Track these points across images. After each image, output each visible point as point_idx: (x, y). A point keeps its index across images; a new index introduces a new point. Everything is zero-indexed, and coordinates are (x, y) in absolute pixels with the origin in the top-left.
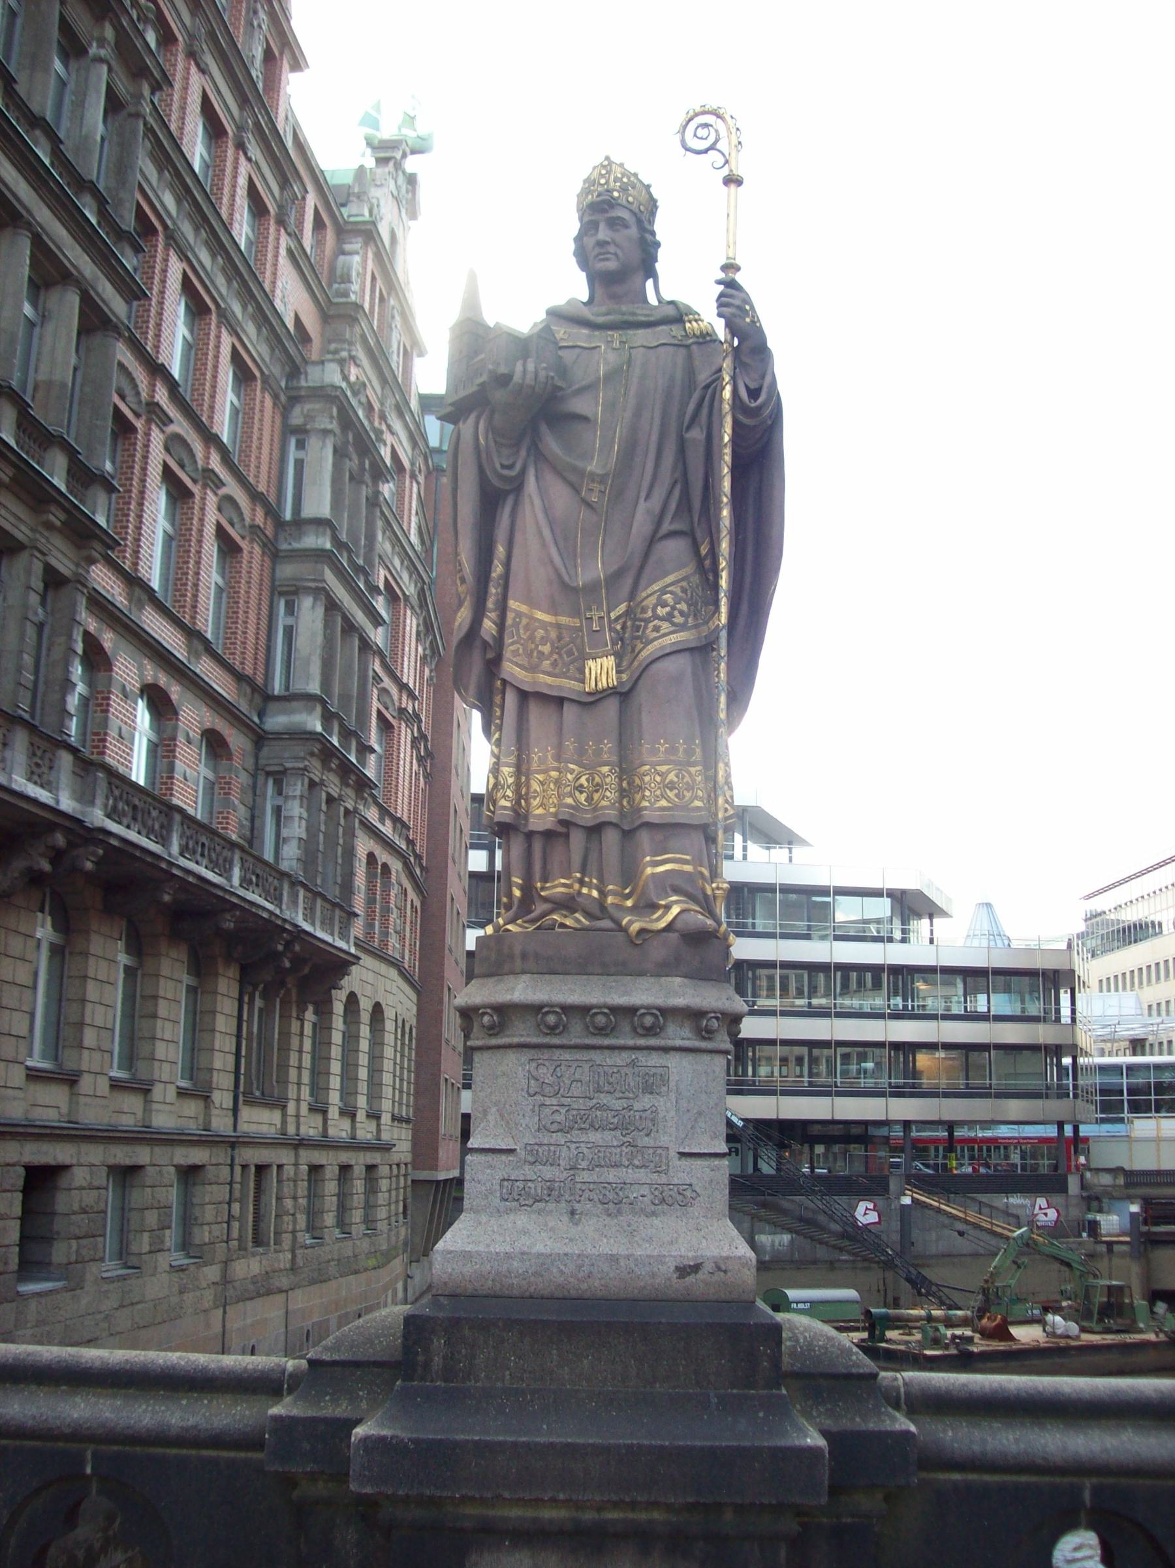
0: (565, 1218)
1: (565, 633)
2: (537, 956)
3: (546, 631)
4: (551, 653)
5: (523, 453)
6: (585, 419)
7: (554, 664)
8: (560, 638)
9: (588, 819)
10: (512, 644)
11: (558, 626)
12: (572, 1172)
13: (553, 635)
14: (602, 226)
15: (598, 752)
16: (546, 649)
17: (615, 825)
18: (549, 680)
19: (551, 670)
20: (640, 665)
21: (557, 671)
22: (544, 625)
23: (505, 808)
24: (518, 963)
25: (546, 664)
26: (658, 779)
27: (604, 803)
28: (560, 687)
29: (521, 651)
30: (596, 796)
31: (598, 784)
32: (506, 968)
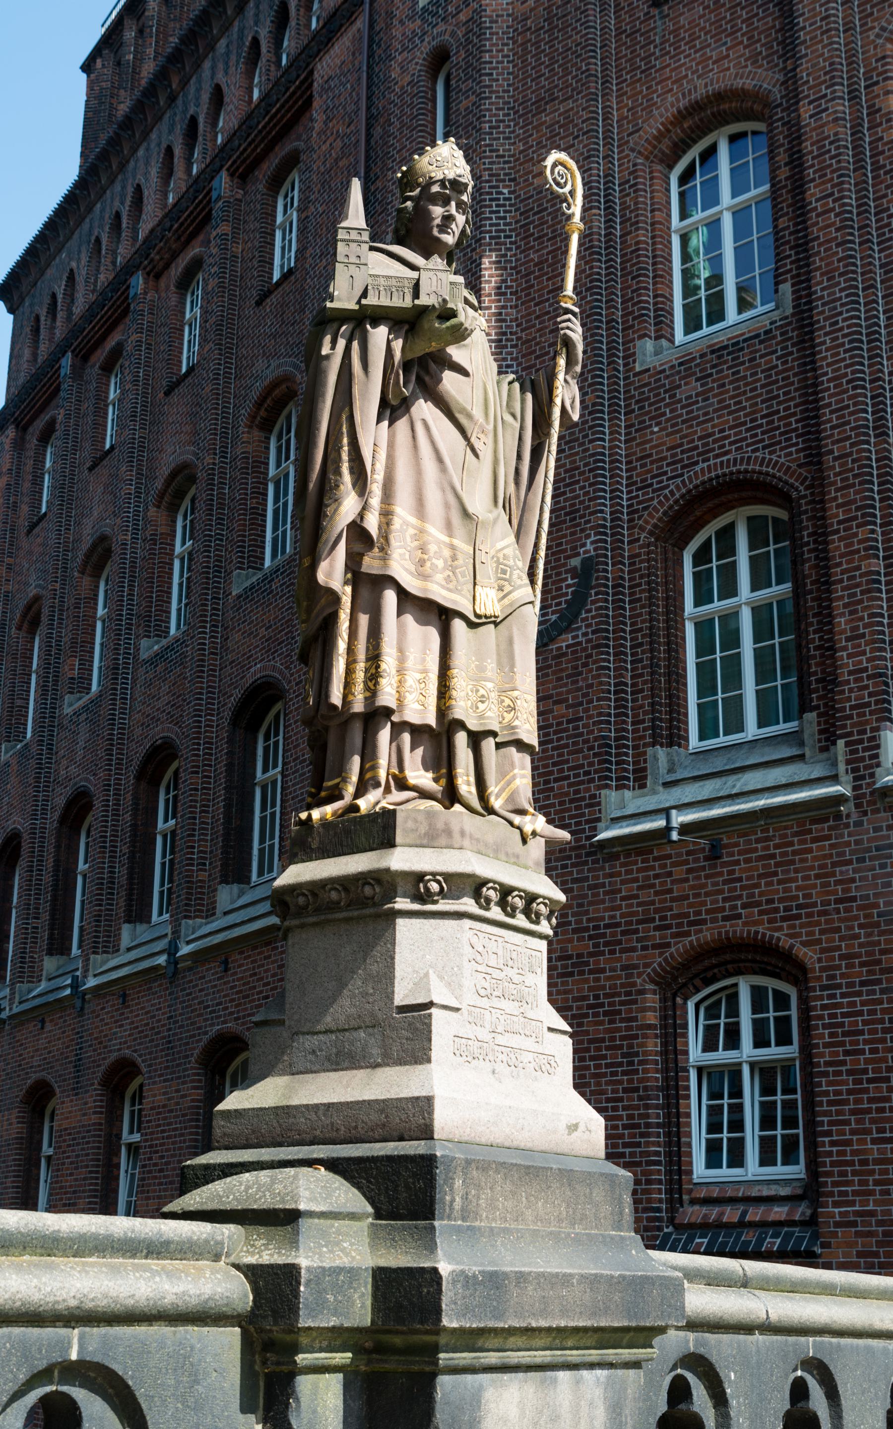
0: (491, 1075)
1: (460, 556)
2: (471, 837)
3: (439, 548)
4: (444, 569)
5: (414, 378)
6: (464, 372)
7: (448, 579)
8: (454, 558)
9: (473, 724)
10: (400, 547)
11: (453, 547)
12: (493, 1035)
13: (447, 553)
14: (453, 204)
15: (481, 669)
16: (440, 563)
17: (494, 734)
18: (444, 593)
19: (444, 583)
20: (511, 605)
21: (451, 586)
22: (439, 542)
23: (391, 695)
24: (457, 840)
25: (439, 577)
26: (525, 705)
27: (489, 714)
28: (455, 602)
29: (407, 557)
30: (482, 706)
31: (483, 696)
32: (443, 841)
